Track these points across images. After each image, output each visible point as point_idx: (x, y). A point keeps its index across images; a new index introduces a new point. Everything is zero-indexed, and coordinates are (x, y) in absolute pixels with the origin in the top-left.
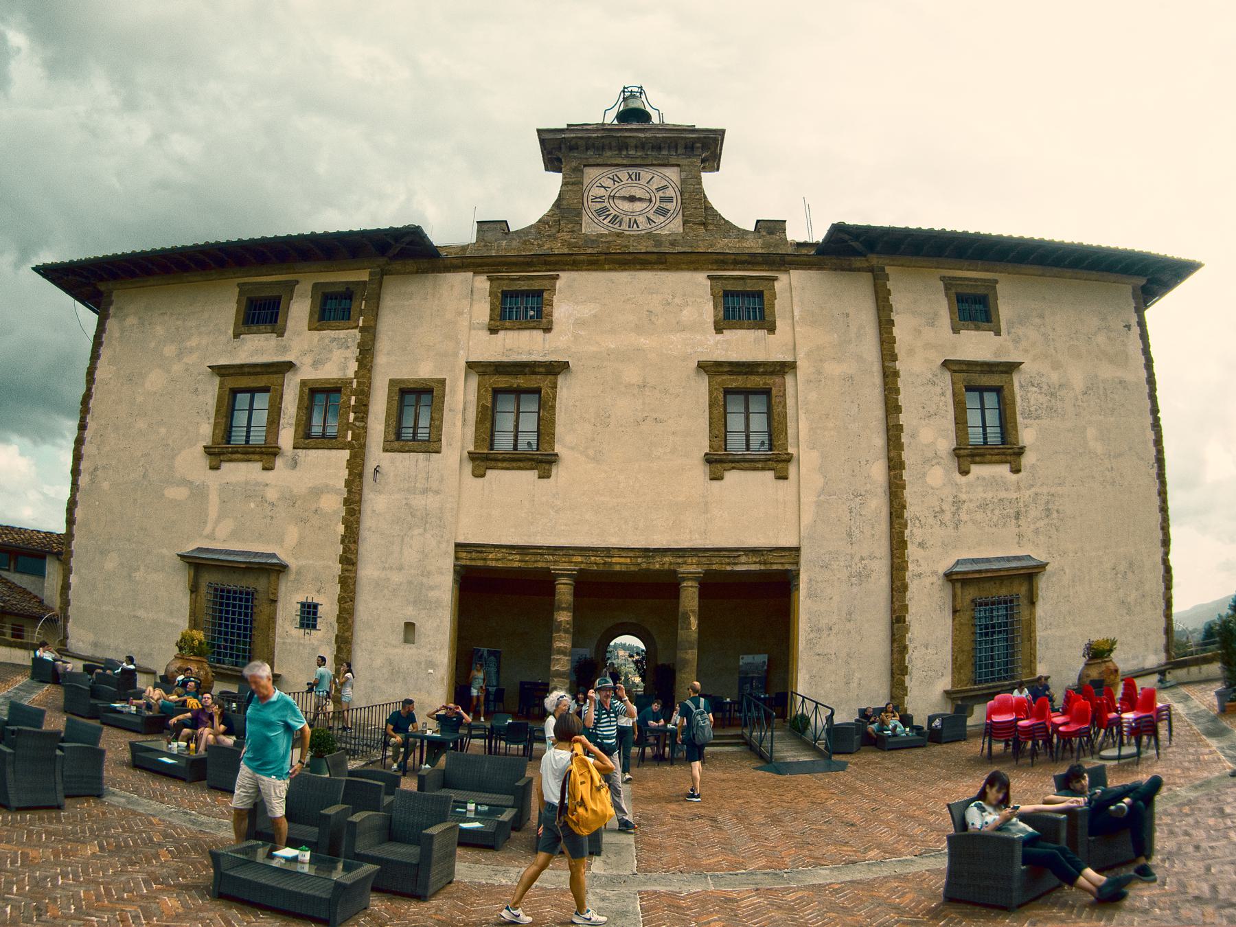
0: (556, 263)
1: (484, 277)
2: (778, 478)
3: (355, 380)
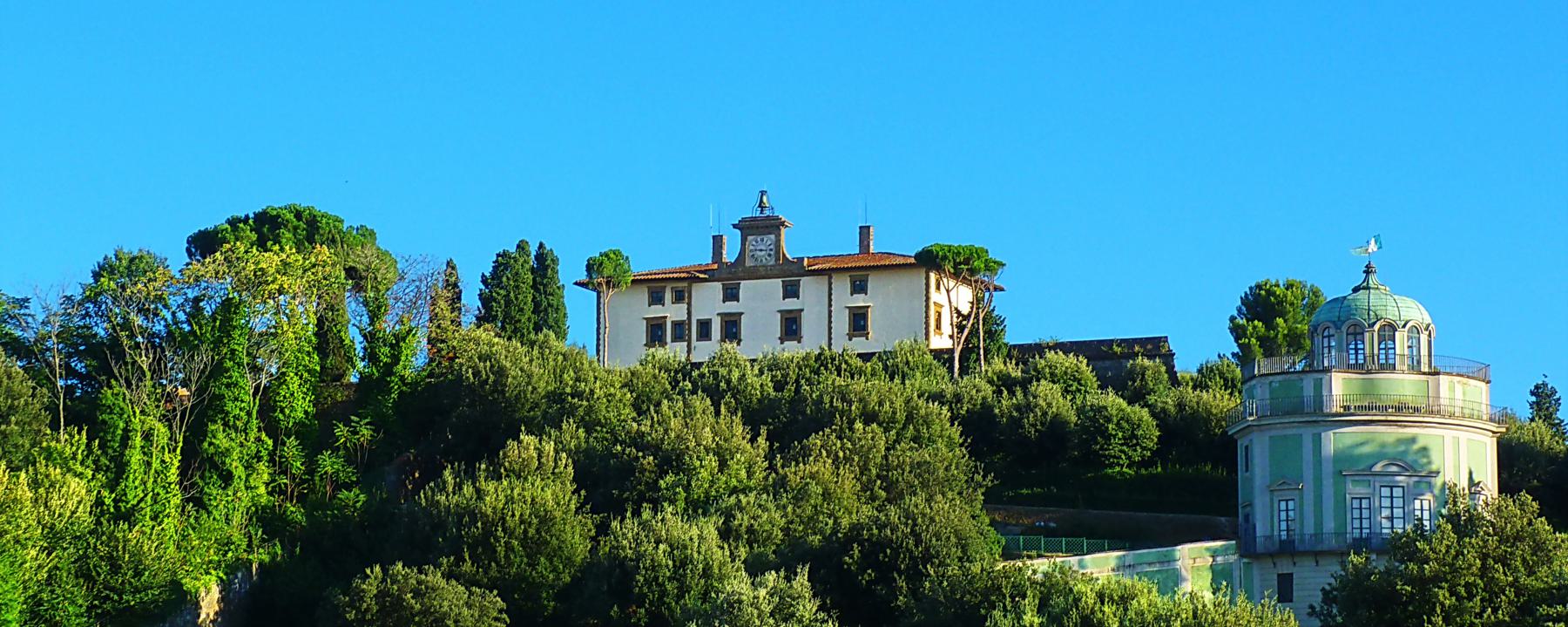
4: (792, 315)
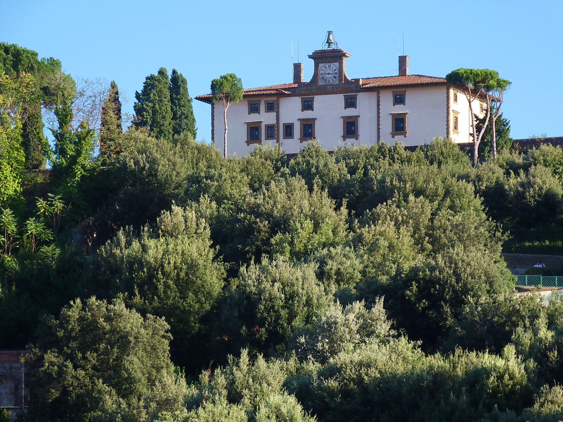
4: (351, 120)
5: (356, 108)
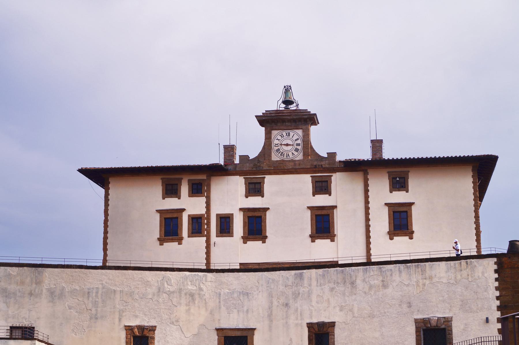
0: (264, 173)
1: (243, 177)
2: (331, 241)
3: (206, 215)
5: (330, 195)
